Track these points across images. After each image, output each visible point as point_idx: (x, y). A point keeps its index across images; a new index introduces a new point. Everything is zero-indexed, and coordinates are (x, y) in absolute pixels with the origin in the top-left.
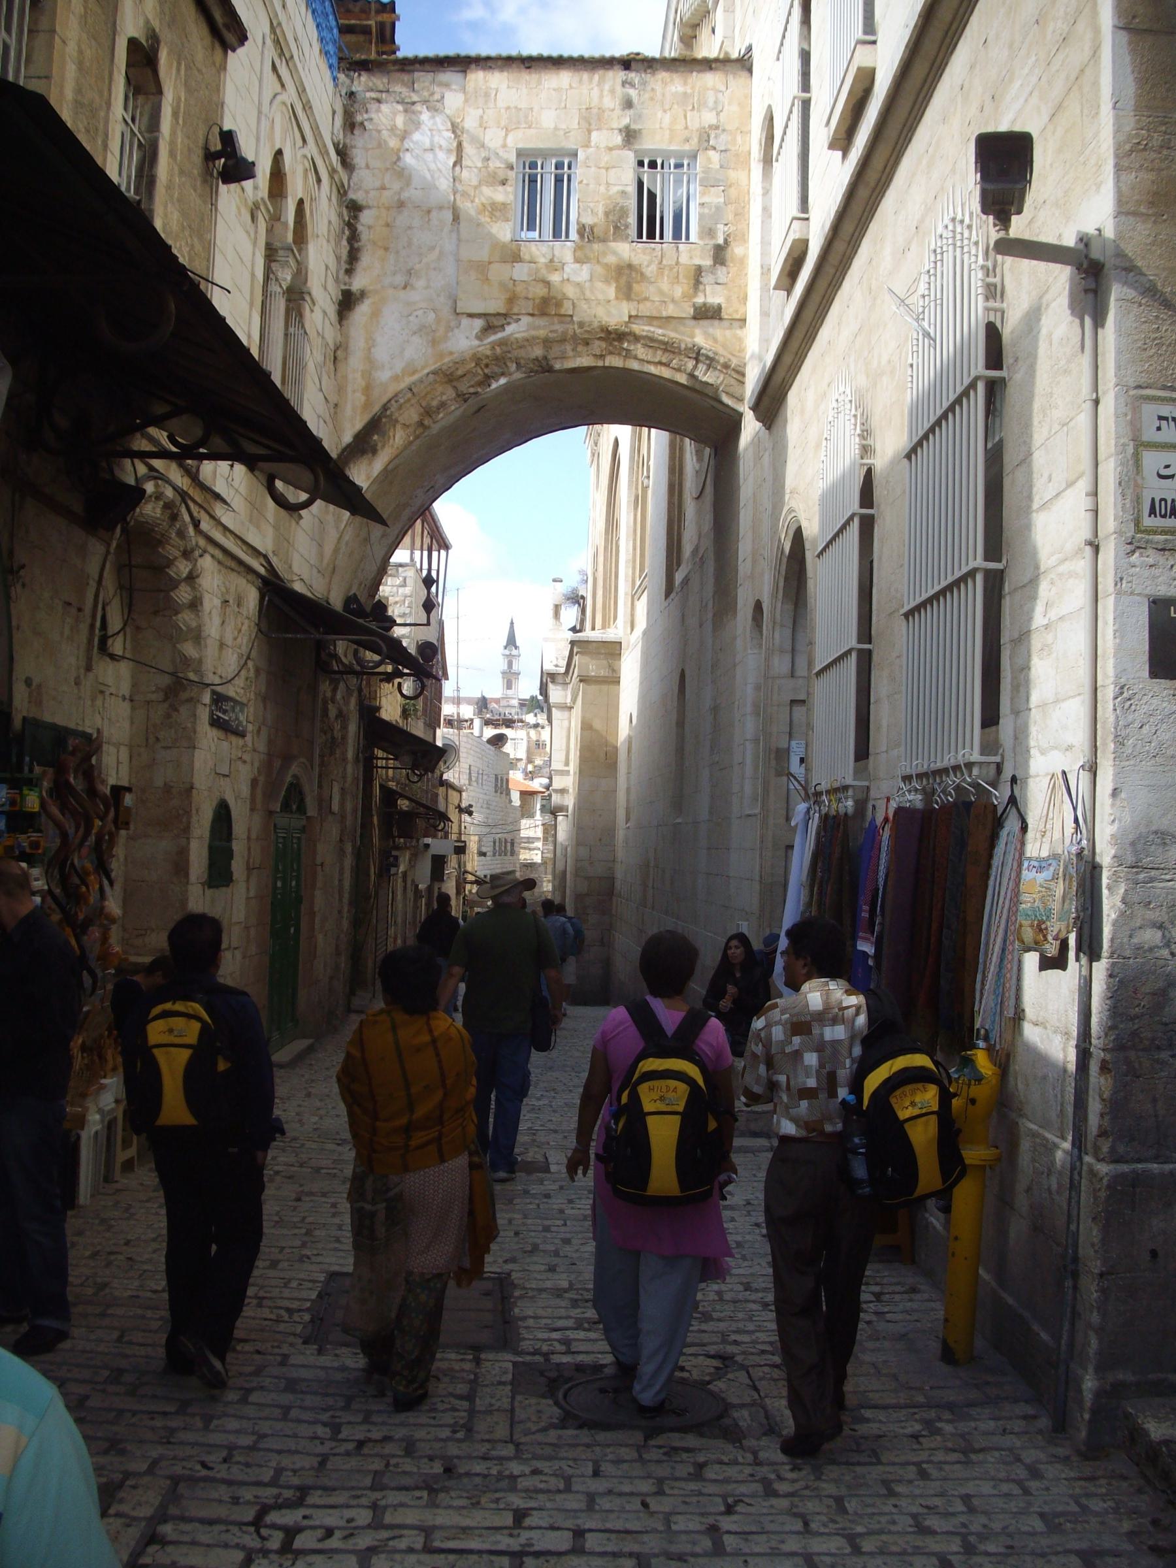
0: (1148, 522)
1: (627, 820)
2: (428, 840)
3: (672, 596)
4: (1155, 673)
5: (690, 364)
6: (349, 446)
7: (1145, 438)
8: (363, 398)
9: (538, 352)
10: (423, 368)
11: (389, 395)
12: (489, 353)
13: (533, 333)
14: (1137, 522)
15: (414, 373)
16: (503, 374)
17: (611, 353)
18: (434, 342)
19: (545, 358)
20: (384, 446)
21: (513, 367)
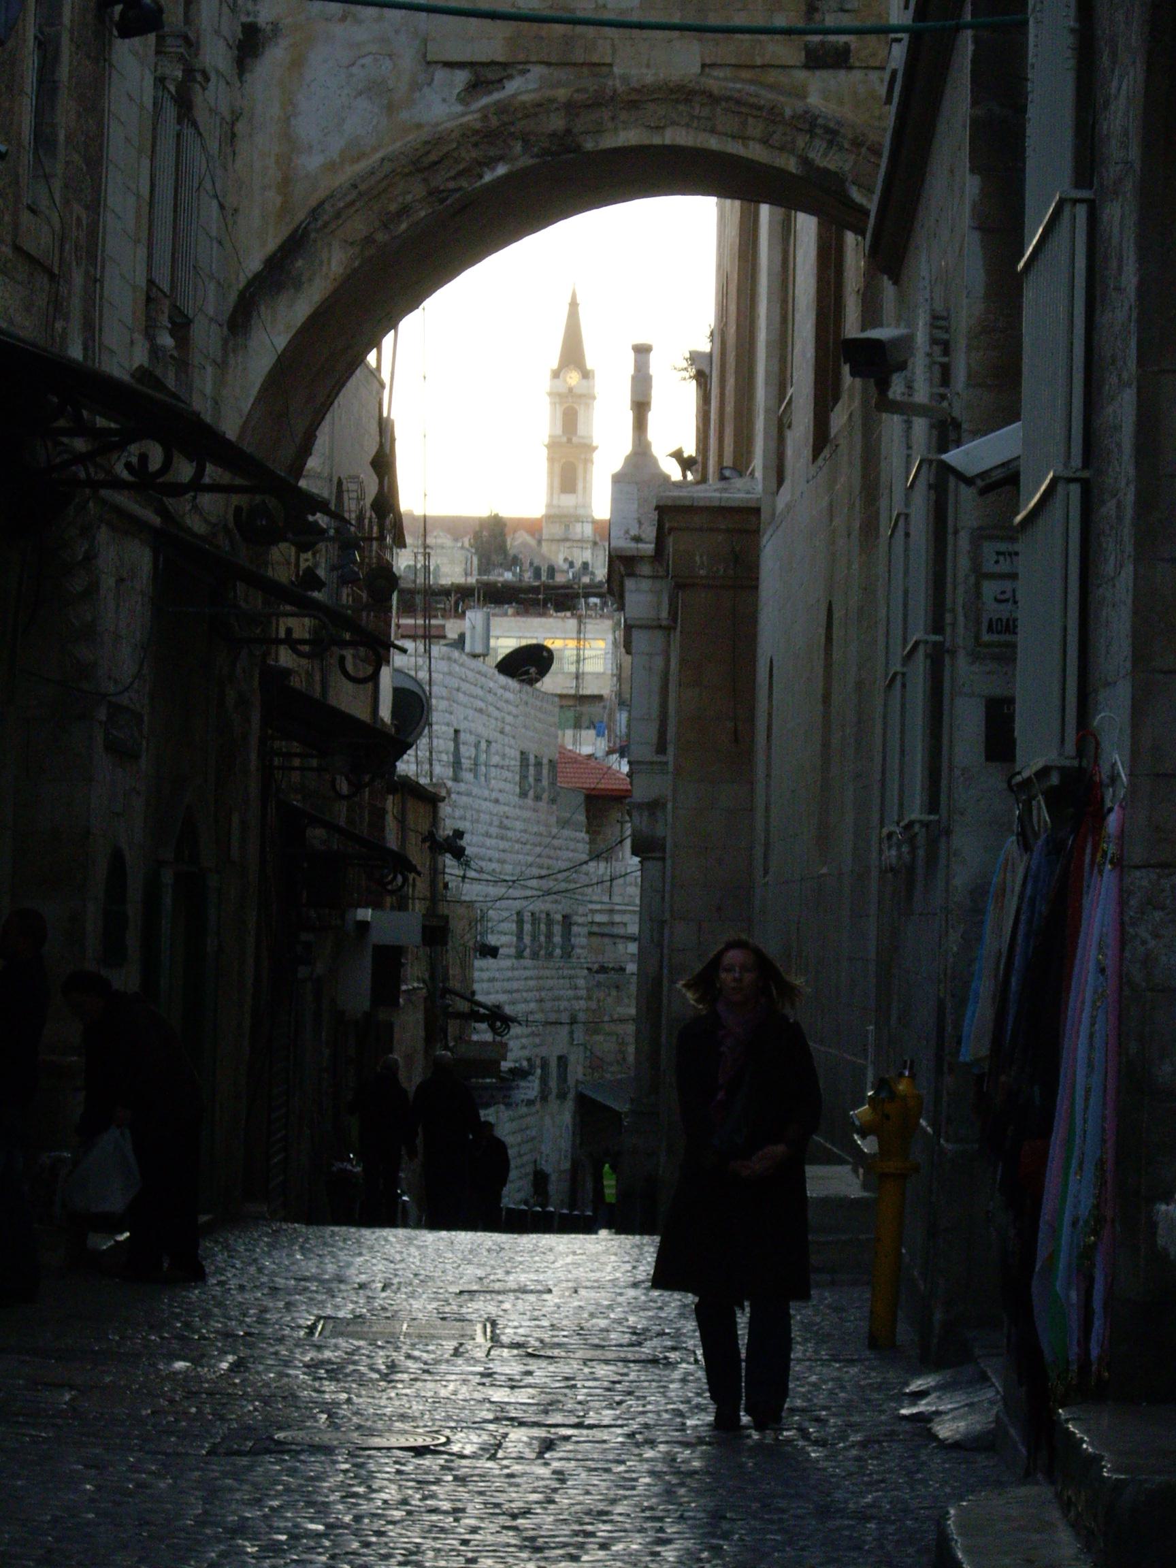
0: (986, 638)
1: (766, 872)
2: (365, 914)
3: (826, 453)
4: (989, 758)
5: (801, 142)
6: (258, 277)
7: (985, 570)
8: (279, 200)
9: (557, 123)
10: (375, 149)
11: (321, 194)
12: (478, 126)
13: (548, 93)
14: (977, 637)
15: (362, 156)
16: (501, 158)
17: (673, 123)
18: (391, 108)
19: (568, 131)
20: (310, 280)
21: (518, 147)
